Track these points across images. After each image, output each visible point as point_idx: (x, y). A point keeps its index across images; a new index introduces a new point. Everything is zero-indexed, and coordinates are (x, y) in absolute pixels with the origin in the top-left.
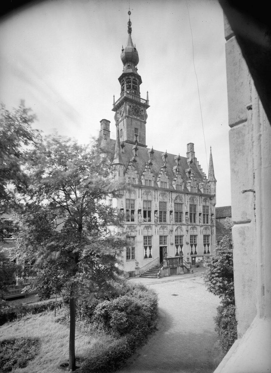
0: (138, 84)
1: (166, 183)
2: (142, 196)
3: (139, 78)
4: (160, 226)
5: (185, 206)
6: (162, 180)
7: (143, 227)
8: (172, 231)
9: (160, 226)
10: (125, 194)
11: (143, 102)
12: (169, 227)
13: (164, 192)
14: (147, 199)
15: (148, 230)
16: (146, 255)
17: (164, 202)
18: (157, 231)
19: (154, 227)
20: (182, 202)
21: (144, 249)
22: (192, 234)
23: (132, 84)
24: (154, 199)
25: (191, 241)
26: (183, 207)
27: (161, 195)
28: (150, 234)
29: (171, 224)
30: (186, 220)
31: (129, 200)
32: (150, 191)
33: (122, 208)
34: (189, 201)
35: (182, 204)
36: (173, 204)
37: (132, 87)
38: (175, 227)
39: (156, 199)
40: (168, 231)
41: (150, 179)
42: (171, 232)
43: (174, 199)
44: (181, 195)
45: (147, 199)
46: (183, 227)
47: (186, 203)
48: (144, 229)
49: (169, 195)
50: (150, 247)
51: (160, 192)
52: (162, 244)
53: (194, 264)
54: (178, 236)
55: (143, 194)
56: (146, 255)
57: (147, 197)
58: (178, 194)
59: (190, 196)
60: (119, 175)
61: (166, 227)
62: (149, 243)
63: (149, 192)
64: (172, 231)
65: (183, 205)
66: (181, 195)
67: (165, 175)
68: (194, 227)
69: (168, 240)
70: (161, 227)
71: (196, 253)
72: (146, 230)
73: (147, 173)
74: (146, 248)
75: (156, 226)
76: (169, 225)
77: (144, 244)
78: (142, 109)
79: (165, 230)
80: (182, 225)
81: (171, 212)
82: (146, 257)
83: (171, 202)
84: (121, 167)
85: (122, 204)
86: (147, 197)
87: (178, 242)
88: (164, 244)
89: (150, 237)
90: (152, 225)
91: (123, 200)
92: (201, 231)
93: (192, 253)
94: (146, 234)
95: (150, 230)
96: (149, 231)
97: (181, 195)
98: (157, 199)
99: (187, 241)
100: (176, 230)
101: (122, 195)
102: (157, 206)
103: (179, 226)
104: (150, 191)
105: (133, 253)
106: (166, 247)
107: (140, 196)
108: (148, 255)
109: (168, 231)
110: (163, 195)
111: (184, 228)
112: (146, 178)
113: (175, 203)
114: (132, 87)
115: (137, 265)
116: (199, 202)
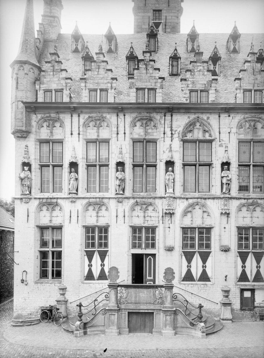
1: (154, 90)
2: (81, 129)
4: (132, 201)
5: (221, 146)
6: (140, 85)
7: (80, 205)
8: (173, 213)
9: (132, 201)
10: (34, 130)
12: (161, 205)
13: (145, 114)
14: (98, 136)
15: (97, 213)
16: (90, 271)
17: (148, 141)
18: (121, 215)
19: (112, 204)
20: (210, 135)
21: (86, 257)
22: (247, 222)
24: (115, 135)
26: (213, 150)
27: (138, 124)
28: (102, 222)
29: (167, 195)
30: (222, 184)
31: (47, 142)
32: (104, 115)
33: (26, 161)
34: (234, 130)
35: (210, 142)
36: (177, 144)
38: (180, 206)
39: (121, 135)
40: (157, 215)
41: (103, 87)
42: (167, 218)
43: (181, 129)
44: (206, 118)
45: (98, 136)
46: (209, 202)
47: (224, 137)
49: (163, 122)
50: (103, 255)
51: (134, 115)
52: (140, 246)
53: (250, 310)
54: (193, 229)
55: (86, 125)
56: (90, 271)
57: (98, 132)
58: (193, 116)
59: (238, 118)
60: (17, 88)
61: (151, 204)
62: (100, 245)
63: (103, 119)
64: (173, 213)
65: (214, 143)
66: (204, 117)
67: (151, 71)
68: (252, 204)
69: (157, 238)
70: (137, 204)
72: (91, 212)
73: (96, 73)
74: (90, 255)
75: (118, 202)
76: (161, 198)
77: (87, 246)
79: (150, 212)
80: (205, 199)
81: (170, 164)
82: (90, 276)
83: (168, 140)
84: (22, 68)
85: (27, 152)
86: (98, 132)
87: (193, 246)
88: (147, 246)
89: (104, 230)
90: (110, 198)
91: (31, 142)
93: (243, 277)
94: (91, 220)
95: (103, 212)
96: (100, 214)
97: (206, 118)
98: (125, 133)
99: (225, 243)
100: (186, 213)
101: (23, 131)
102: (124, 151)
103: (195, 200)
104: (104, 115)
105: (44, 264)
106: (154, 255)
107: (75, 133)
108: (96, 273)
109: (157, 215)
110: (147, 121)
111: (215, 207)
112: (92, 87)
113: (184, 141)
115: (63, 294)
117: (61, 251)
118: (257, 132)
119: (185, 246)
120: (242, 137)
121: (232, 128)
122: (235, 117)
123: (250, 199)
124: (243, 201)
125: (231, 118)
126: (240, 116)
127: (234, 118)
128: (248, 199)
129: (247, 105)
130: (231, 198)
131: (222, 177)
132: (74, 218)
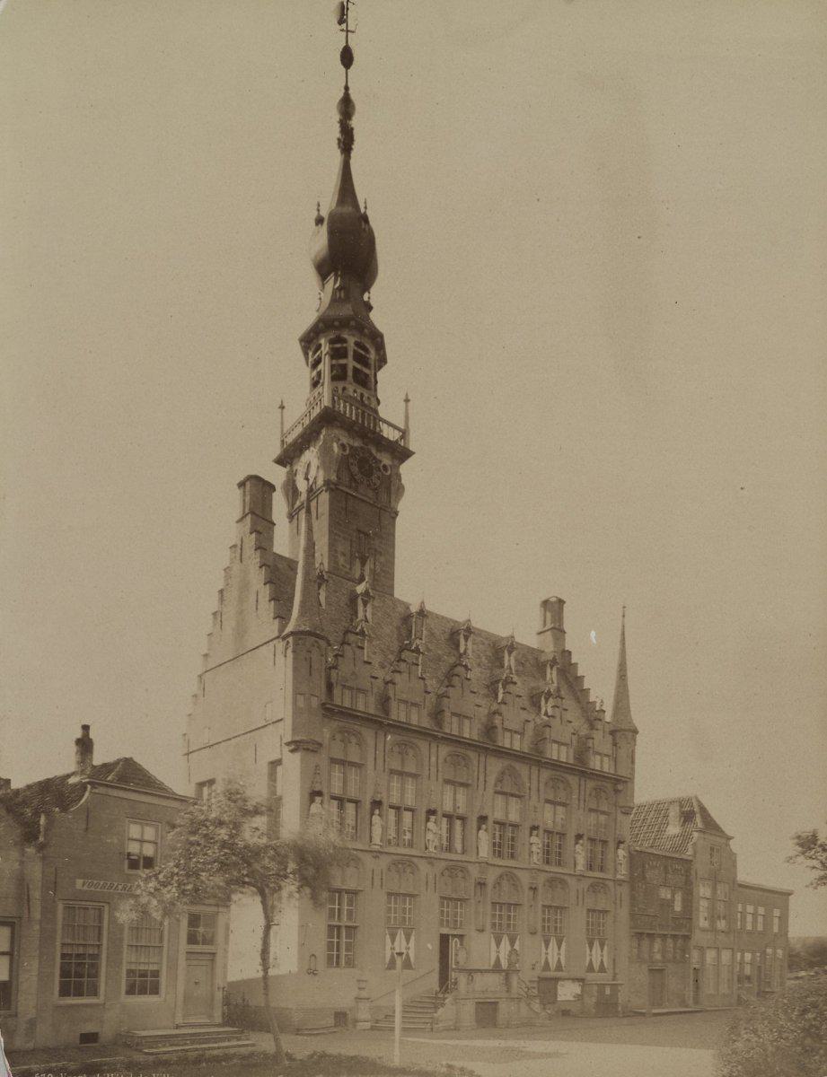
0: (373, 367)
3: (377, 339)
11: (390, 434)
19: (423, 867)
23: (351, 363)
25: (544, 927)
37: (350, 373)
48: (389, 869)
71: (559, 968)
78: (386, 460)
100: (498, 884)
106: (461, 937)
114: (350, 373)
117: (356, 927)
119: (494, 925)
131: (531, 844)
132: (377, 882)
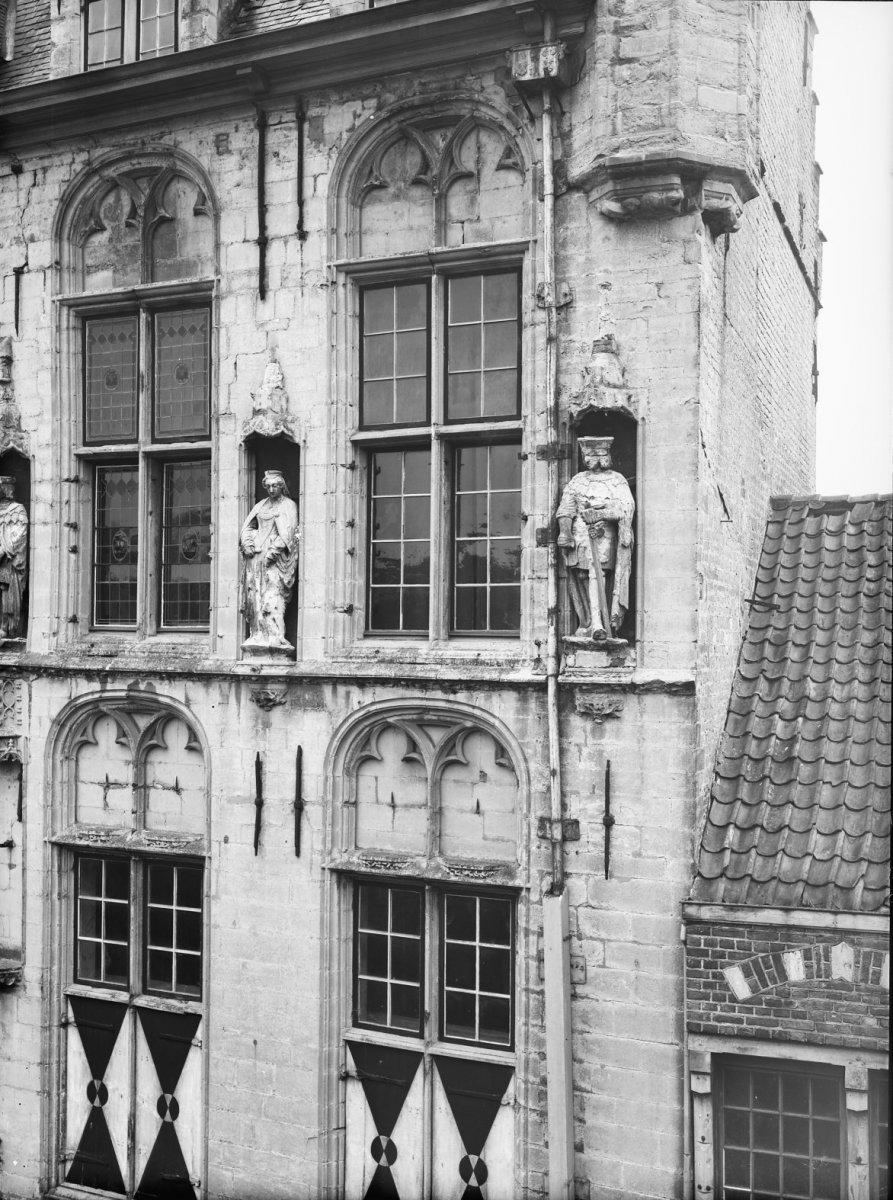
34: (42, 253)
92: (279, 792)
116: (238, 225)
118: (174, 242)
120: (101, 284)
121: (32, 239)
122: (45, 170)
123: (115, 674)
124: (85, 689)
125: (26, 179)
126: (67, 159)
127: (40, 176)
128: (103, 676)
129: (49, 94)
130: (22, 671)
